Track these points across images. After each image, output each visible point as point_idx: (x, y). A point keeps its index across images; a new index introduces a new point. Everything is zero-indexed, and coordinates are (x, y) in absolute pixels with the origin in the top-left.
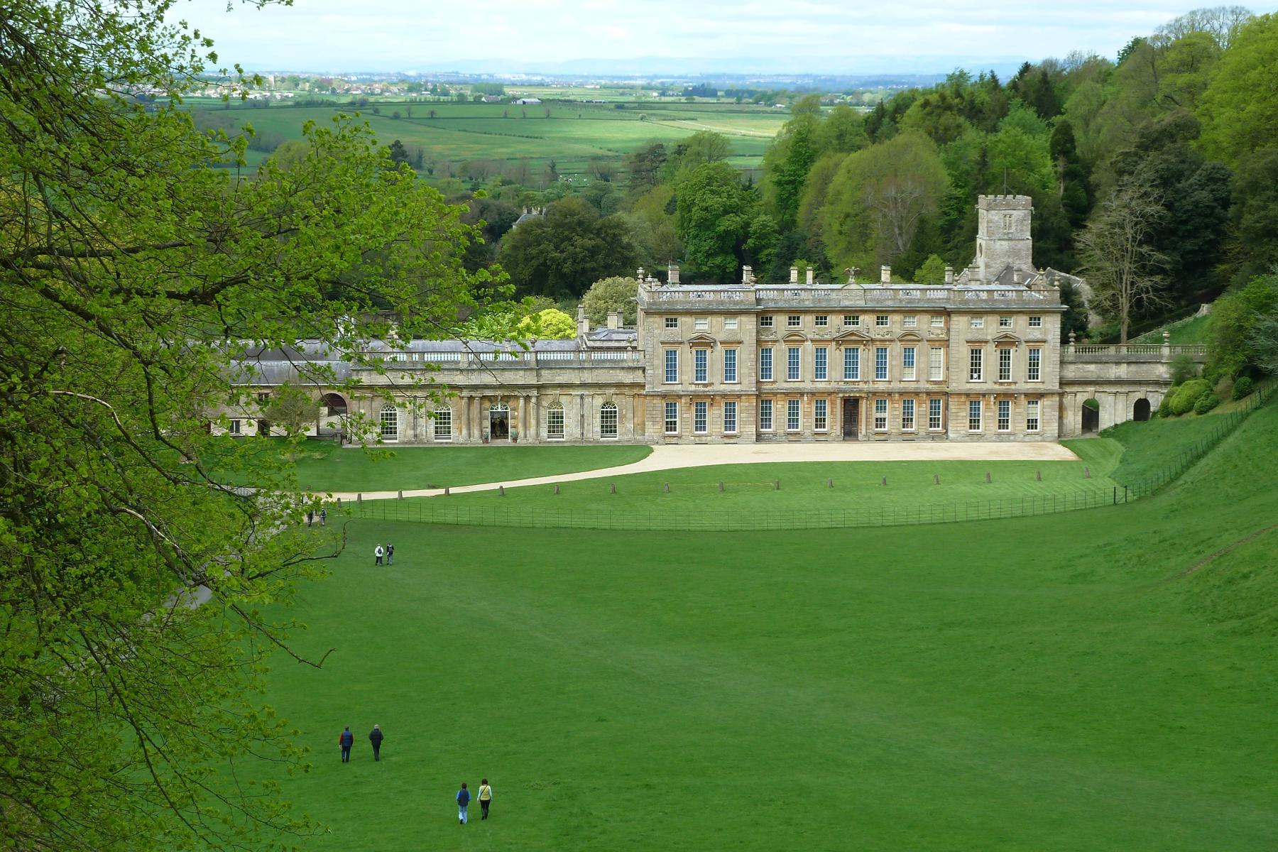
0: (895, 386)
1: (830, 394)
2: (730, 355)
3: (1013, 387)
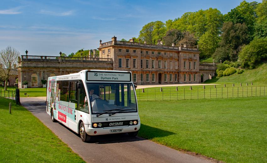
1: (155, 72)
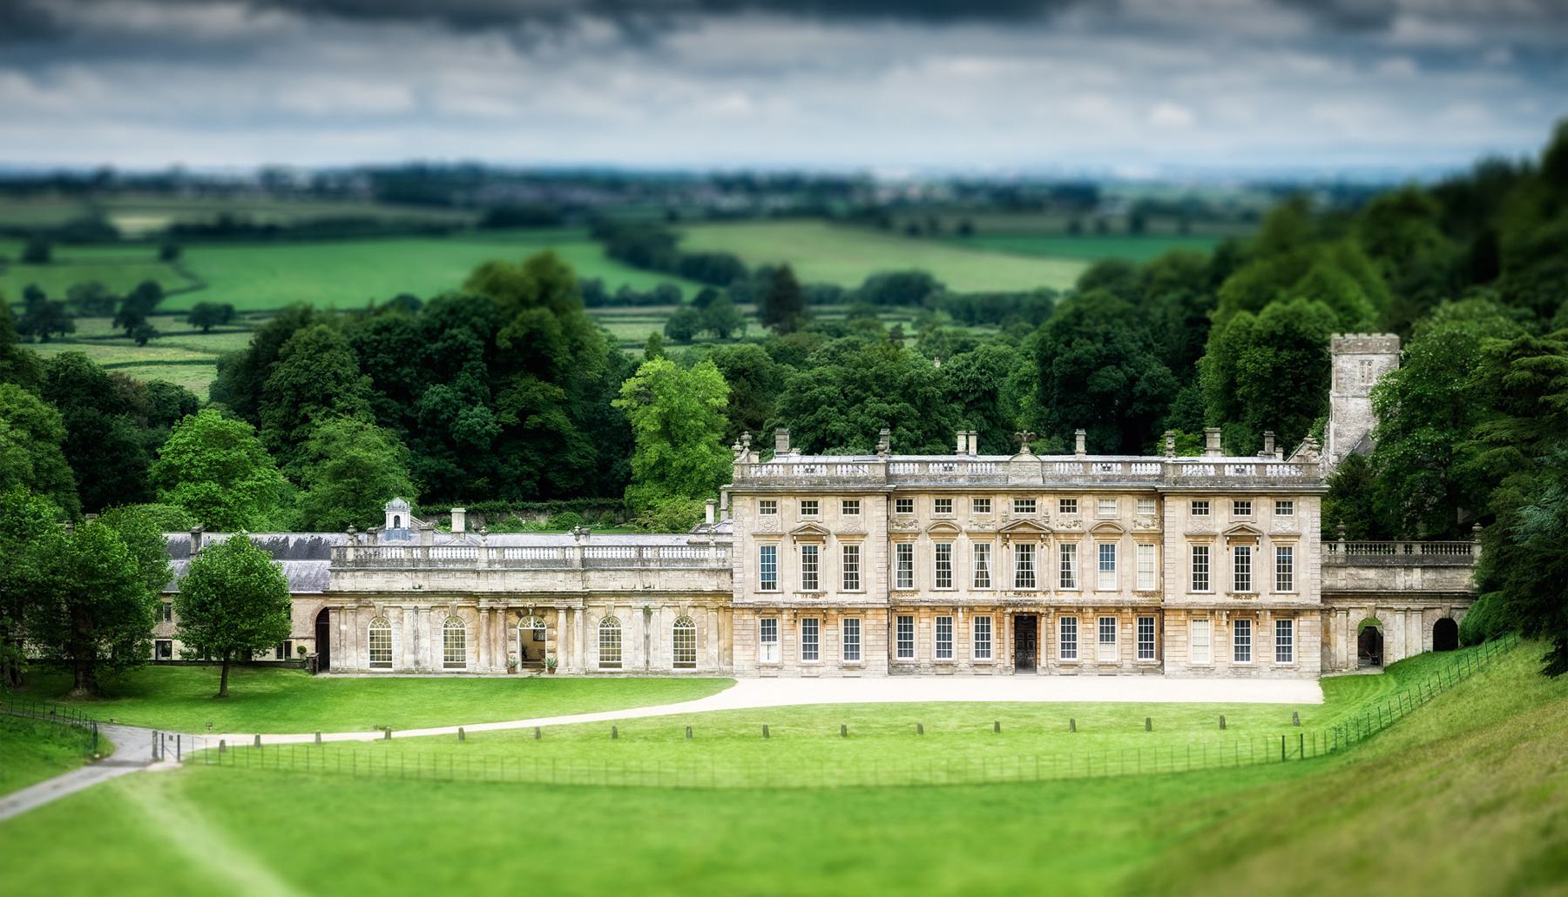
0: (1088, 598)
1: (994, 608)
2: (851, 558)
3: (1254, 600)
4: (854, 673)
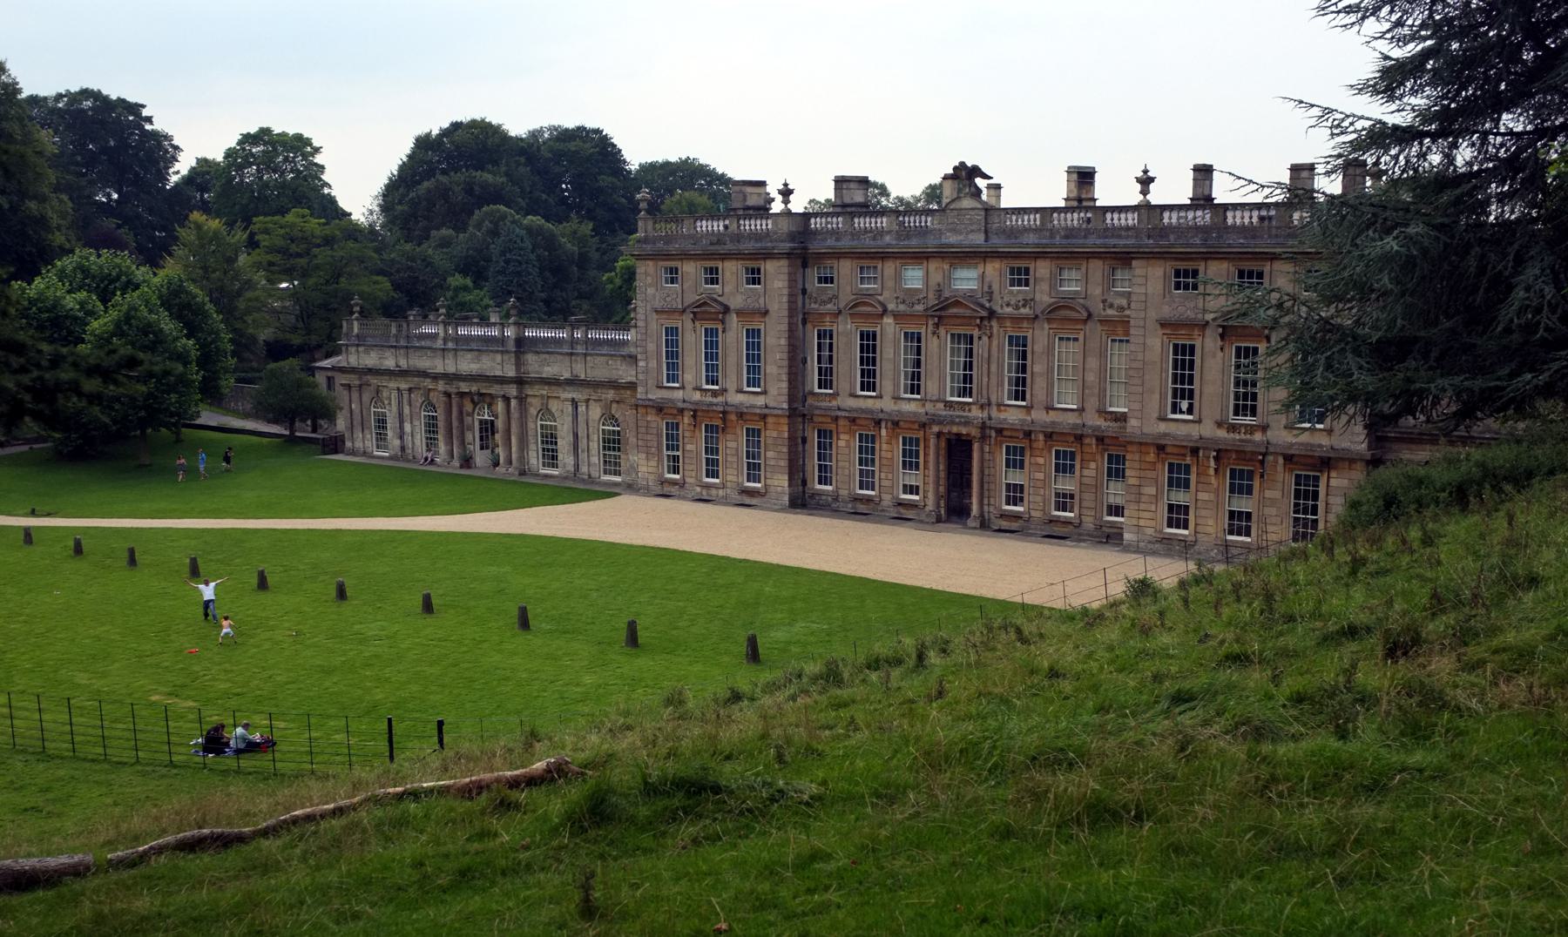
3: (1258, 437)
4: (754, 501)
